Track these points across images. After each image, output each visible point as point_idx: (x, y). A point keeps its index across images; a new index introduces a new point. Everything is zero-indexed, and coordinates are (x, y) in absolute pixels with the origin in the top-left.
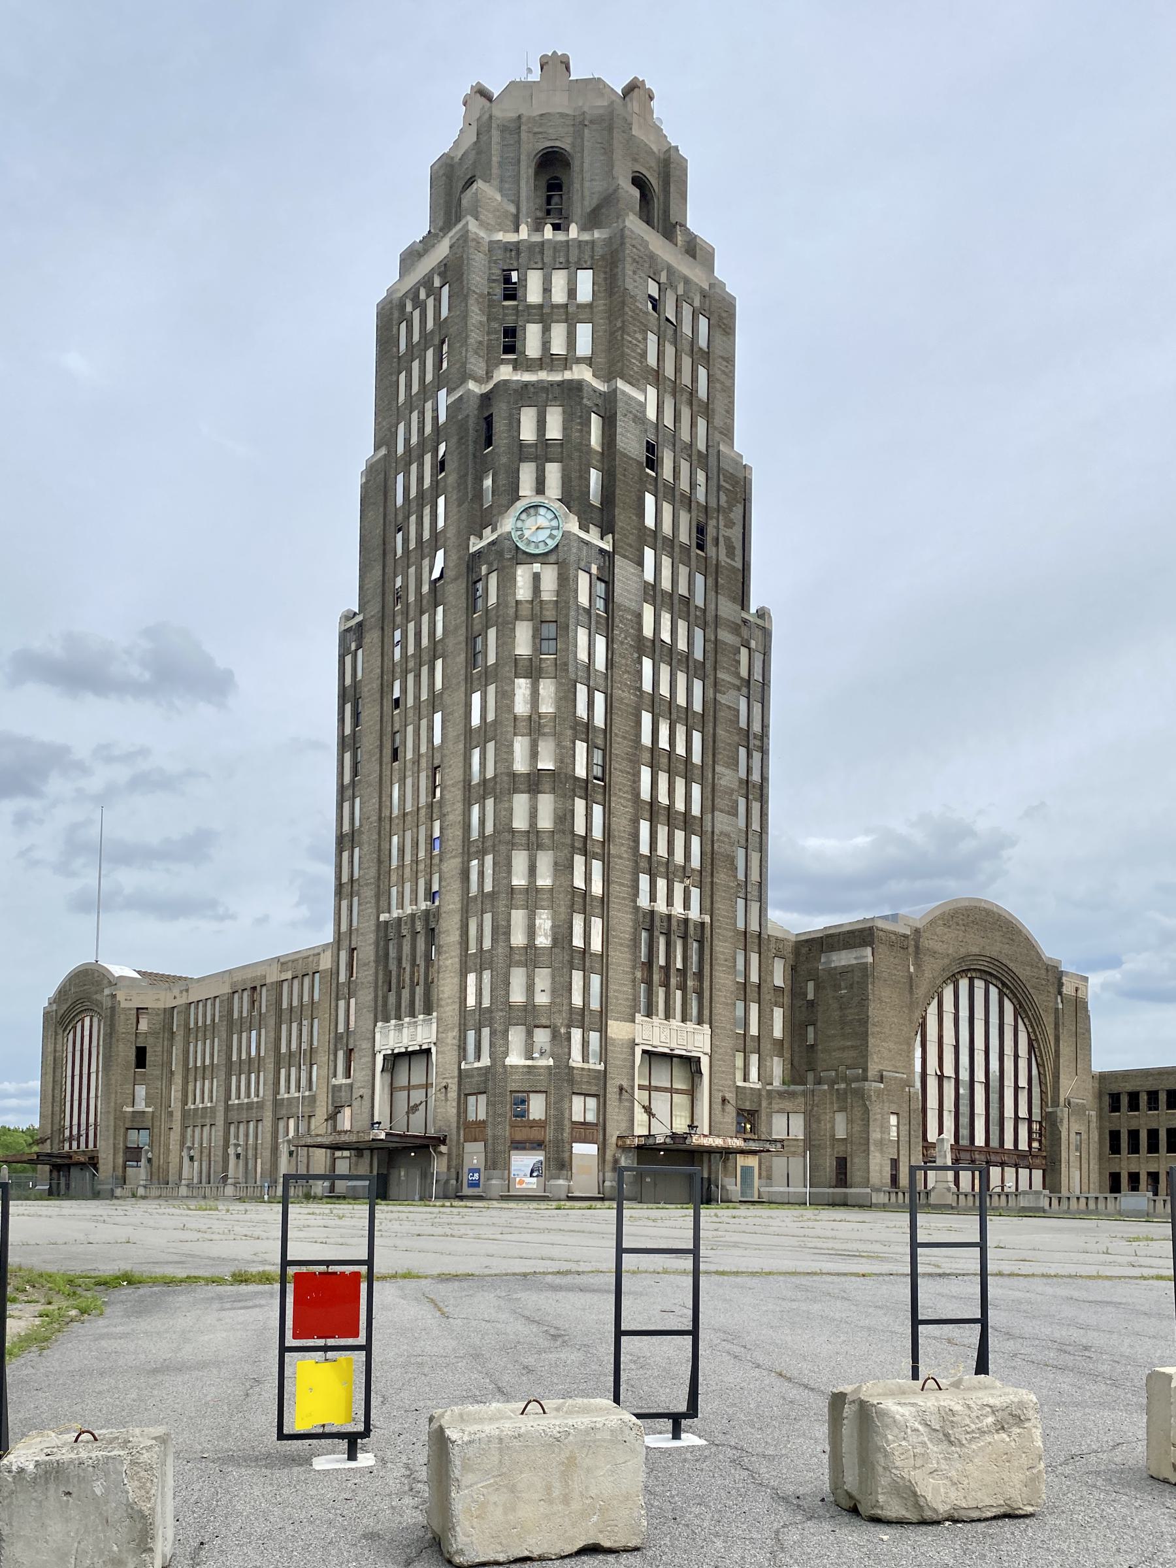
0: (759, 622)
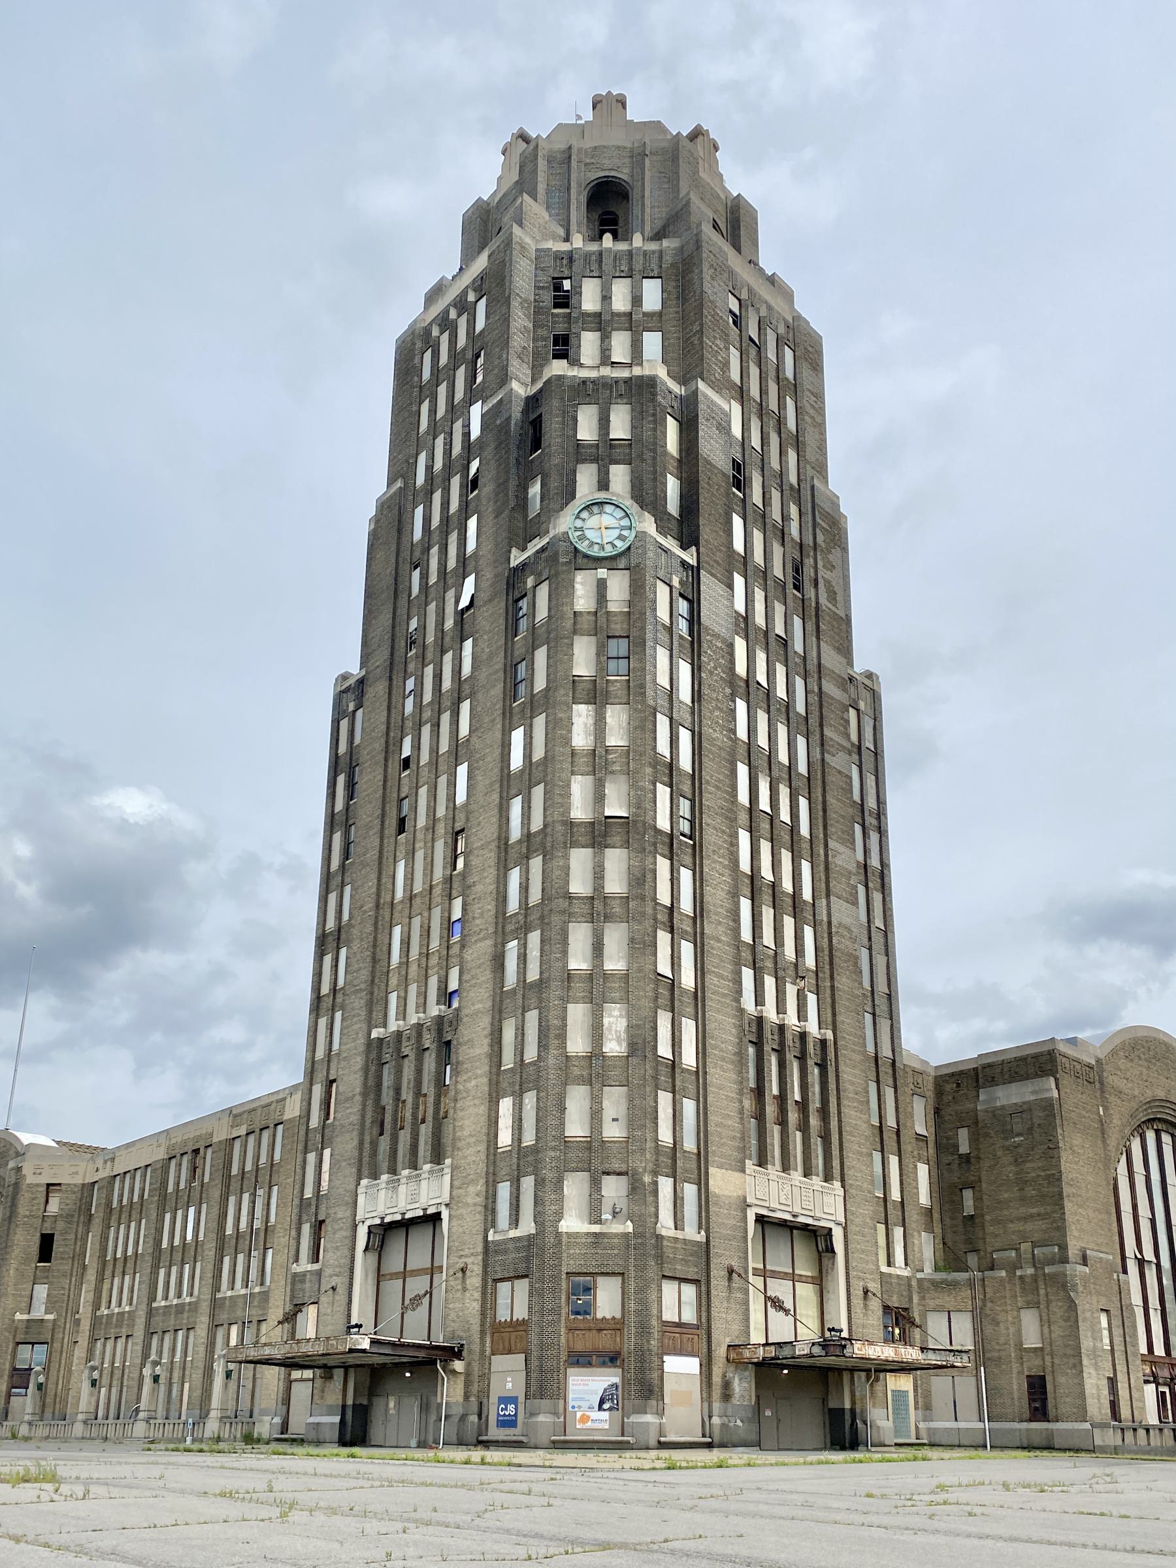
0: (867, 682)
